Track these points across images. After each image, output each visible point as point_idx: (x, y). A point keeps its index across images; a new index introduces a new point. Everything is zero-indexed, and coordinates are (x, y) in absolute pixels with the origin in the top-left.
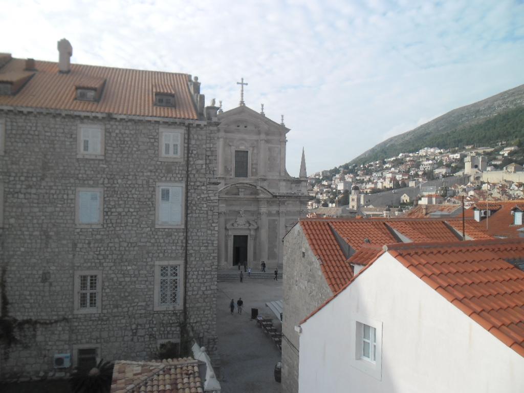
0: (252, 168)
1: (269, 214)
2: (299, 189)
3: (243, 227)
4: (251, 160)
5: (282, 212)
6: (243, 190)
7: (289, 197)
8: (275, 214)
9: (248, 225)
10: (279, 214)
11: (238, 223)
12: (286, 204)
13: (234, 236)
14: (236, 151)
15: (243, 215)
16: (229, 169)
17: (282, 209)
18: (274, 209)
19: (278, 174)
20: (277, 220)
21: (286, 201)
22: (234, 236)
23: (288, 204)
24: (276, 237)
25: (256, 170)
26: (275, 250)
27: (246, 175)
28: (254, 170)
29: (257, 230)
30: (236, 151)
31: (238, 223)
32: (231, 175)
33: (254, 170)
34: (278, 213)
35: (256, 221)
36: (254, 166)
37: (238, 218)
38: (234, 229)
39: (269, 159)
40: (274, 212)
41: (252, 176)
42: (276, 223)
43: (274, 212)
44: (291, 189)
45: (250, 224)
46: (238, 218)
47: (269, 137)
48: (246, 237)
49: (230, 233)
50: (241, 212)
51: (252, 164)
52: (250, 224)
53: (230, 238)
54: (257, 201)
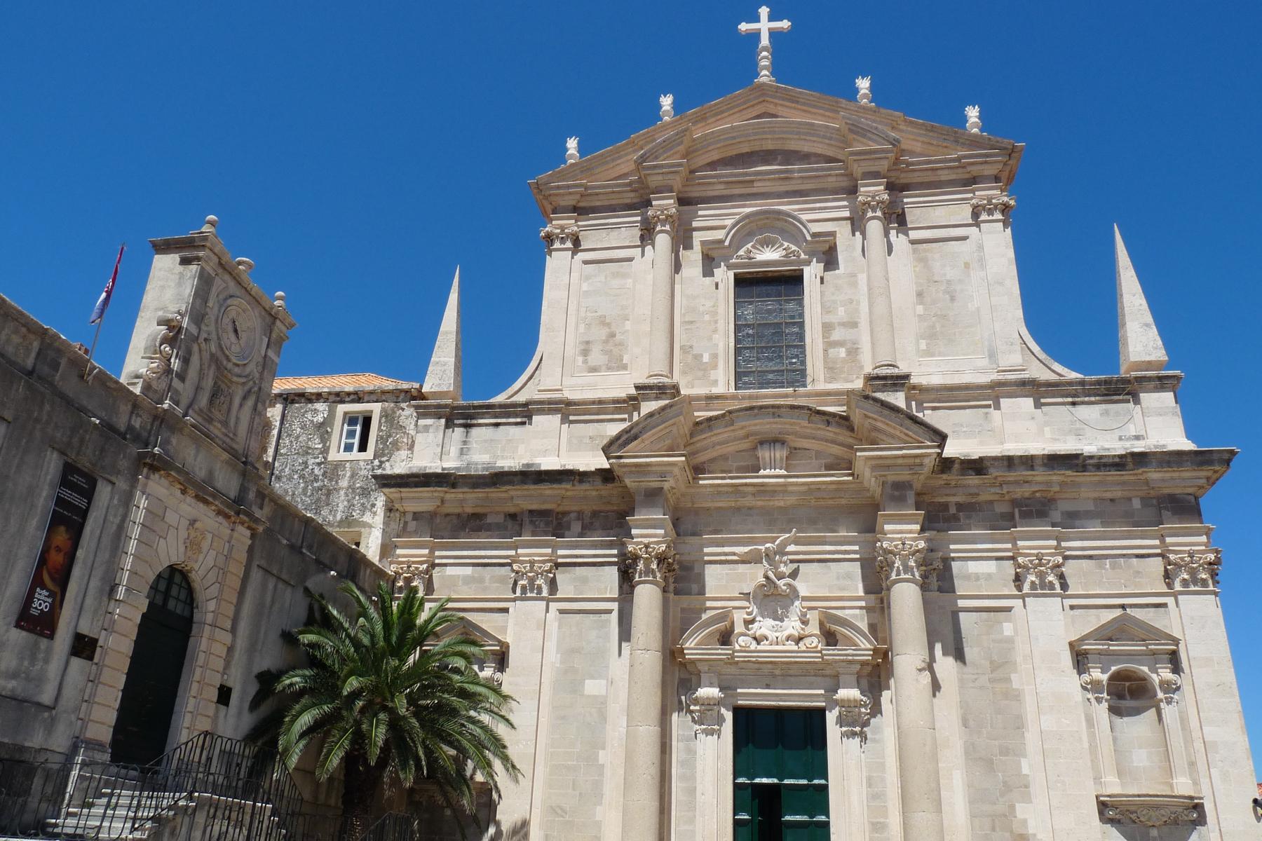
0: (829, 345)
2: (1132, 430)
4: (818, 308)
16: (706, 358)
19: (984, 362)
25: (853, 352)
26: (1021, 811)
27: (798, 376)
28: (842, 352)
32: (715, 382)
33: (842, 352)
36: (836, 335)
39: (920, 294)
41: (829, 380)
44: (1078, 434)
51: (827, 328)
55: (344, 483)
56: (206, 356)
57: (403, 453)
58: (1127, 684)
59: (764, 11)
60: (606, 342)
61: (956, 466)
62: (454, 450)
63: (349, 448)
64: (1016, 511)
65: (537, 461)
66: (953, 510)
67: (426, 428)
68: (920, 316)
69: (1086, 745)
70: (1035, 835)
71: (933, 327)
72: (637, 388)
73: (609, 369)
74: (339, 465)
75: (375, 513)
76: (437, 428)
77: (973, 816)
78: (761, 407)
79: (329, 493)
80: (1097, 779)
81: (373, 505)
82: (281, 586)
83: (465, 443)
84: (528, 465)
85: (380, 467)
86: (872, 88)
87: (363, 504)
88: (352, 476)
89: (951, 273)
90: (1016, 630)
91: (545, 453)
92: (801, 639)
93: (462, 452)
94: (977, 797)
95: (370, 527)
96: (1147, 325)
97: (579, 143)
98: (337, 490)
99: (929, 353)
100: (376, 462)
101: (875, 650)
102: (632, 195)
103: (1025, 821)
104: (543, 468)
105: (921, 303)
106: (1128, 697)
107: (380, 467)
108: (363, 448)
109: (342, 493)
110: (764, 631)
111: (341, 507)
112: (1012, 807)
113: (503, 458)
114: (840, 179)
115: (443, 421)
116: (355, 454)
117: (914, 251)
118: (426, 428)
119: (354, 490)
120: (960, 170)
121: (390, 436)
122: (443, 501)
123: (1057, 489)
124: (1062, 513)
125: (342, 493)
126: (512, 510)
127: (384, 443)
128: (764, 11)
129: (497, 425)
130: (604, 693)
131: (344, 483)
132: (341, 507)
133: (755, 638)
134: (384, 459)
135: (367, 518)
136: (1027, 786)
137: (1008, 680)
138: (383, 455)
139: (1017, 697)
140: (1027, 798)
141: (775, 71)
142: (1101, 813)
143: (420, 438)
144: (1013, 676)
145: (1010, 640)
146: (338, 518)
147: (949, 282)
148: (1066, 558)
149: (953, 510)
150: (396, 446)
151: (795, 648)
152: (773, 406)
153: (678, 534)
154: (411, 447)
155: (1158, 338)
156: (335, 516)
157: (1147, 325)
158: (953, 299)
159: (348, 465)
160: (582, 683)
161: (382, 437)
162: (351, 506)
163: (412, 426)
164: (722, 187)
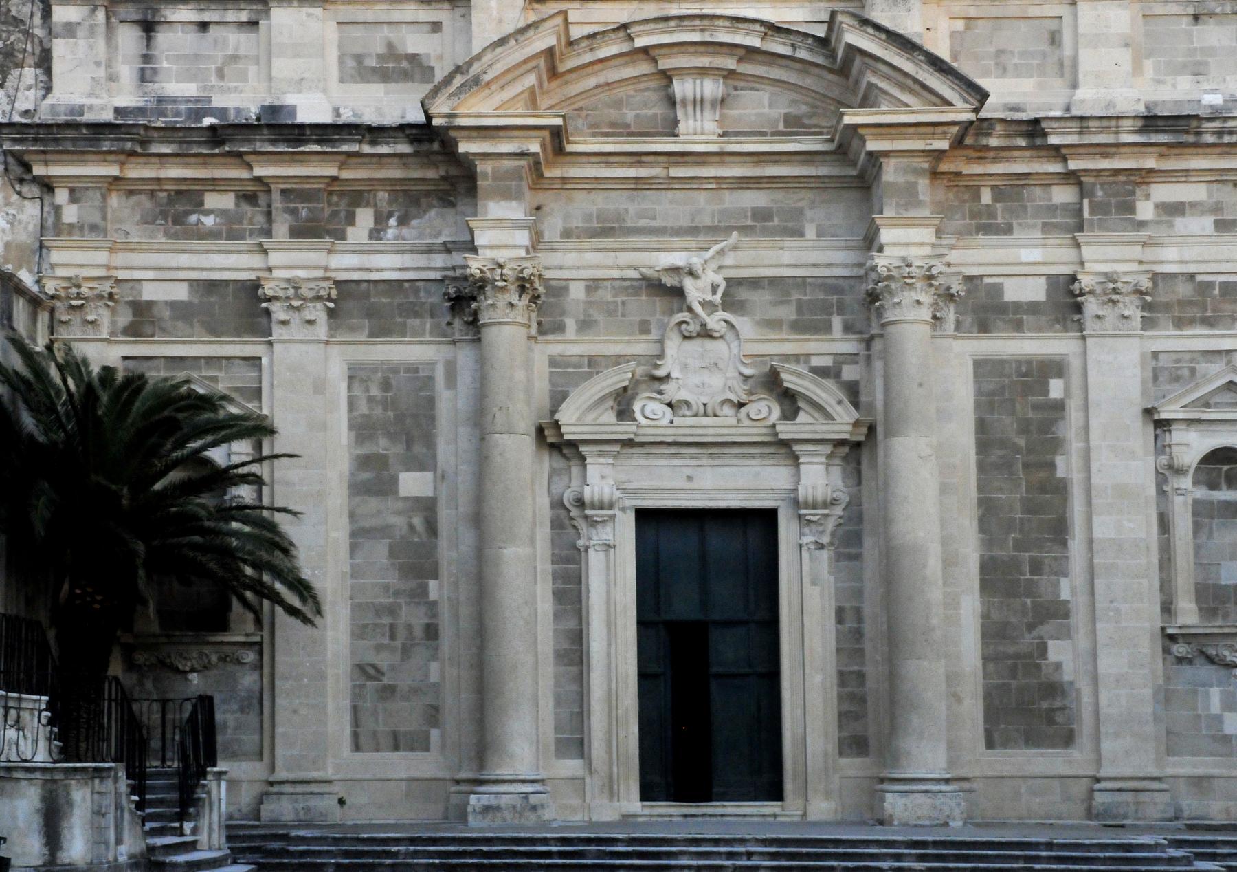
1: (983, 307)
3: (726, 425)
5: (1111, 291)
6: (711, 88)
7: (1172, 128)
8: (1033, 308)
9: (766, 409)
10: (1078, 308)
11: (672, 391)
12: (1145, 210)
13: (645, 517)
15: (715, 321)
17: (1105, 257)
18: (1022, 261)
21: (1145, 177)
22: (645, 517)
23: (1175, 209)
24: (1059, 531)
26: (1057, 651)
29: (858, 451)
31: (672, 391)
34: (1067, 302)
35: (849, 373)
37: (673, 345)
38: (629, 443)
40: (1035, 291)
42: (1056, 389)
43: (1035, 291)
44: (1198, 70)
45: (790, 401)
46: (673, 345)
49: (601, 479)
50: (695, 291)
52: (790, 401)
53: (604, 534)
54: (855, 175)
58: (1225, 468)
62: (127, 72)
64: (1086, 202)
65: (289, 99)
66: (986, 197)
67: (70, 30)
69: (1155, 560)
70: (1071, 683)
77: (986, 659)
80: (1167, 609)
83: (146, 58)
84: (273, 110)
90: (1067, 390)
91: (299, 84)
92: (741, 405)
93: (144, 77)
94: (993, 633)
101: (856, 424)
103: (1058, 666)
104: (303, 117)
106: (1224, 486)
110: (684, 395)
112: (1043, 649)
113: (222, 90)
115: (101, 15)
118: (70, 30)
124: (1157, 206)
129: (204, 26)
130: (429, 493)
133: (670, 405)
136: (1066, 616)
137: (1052, 466)
139: (1061, 489)
140: (1066, 634)
142: (1166, 651)
143: (59, 48)
144: (1059, 460)
145: (1059, 407)
148: (1155, 277)
151: (733, 421)
154: (45, 61)
160: (394, 481)
163: (37, 20)
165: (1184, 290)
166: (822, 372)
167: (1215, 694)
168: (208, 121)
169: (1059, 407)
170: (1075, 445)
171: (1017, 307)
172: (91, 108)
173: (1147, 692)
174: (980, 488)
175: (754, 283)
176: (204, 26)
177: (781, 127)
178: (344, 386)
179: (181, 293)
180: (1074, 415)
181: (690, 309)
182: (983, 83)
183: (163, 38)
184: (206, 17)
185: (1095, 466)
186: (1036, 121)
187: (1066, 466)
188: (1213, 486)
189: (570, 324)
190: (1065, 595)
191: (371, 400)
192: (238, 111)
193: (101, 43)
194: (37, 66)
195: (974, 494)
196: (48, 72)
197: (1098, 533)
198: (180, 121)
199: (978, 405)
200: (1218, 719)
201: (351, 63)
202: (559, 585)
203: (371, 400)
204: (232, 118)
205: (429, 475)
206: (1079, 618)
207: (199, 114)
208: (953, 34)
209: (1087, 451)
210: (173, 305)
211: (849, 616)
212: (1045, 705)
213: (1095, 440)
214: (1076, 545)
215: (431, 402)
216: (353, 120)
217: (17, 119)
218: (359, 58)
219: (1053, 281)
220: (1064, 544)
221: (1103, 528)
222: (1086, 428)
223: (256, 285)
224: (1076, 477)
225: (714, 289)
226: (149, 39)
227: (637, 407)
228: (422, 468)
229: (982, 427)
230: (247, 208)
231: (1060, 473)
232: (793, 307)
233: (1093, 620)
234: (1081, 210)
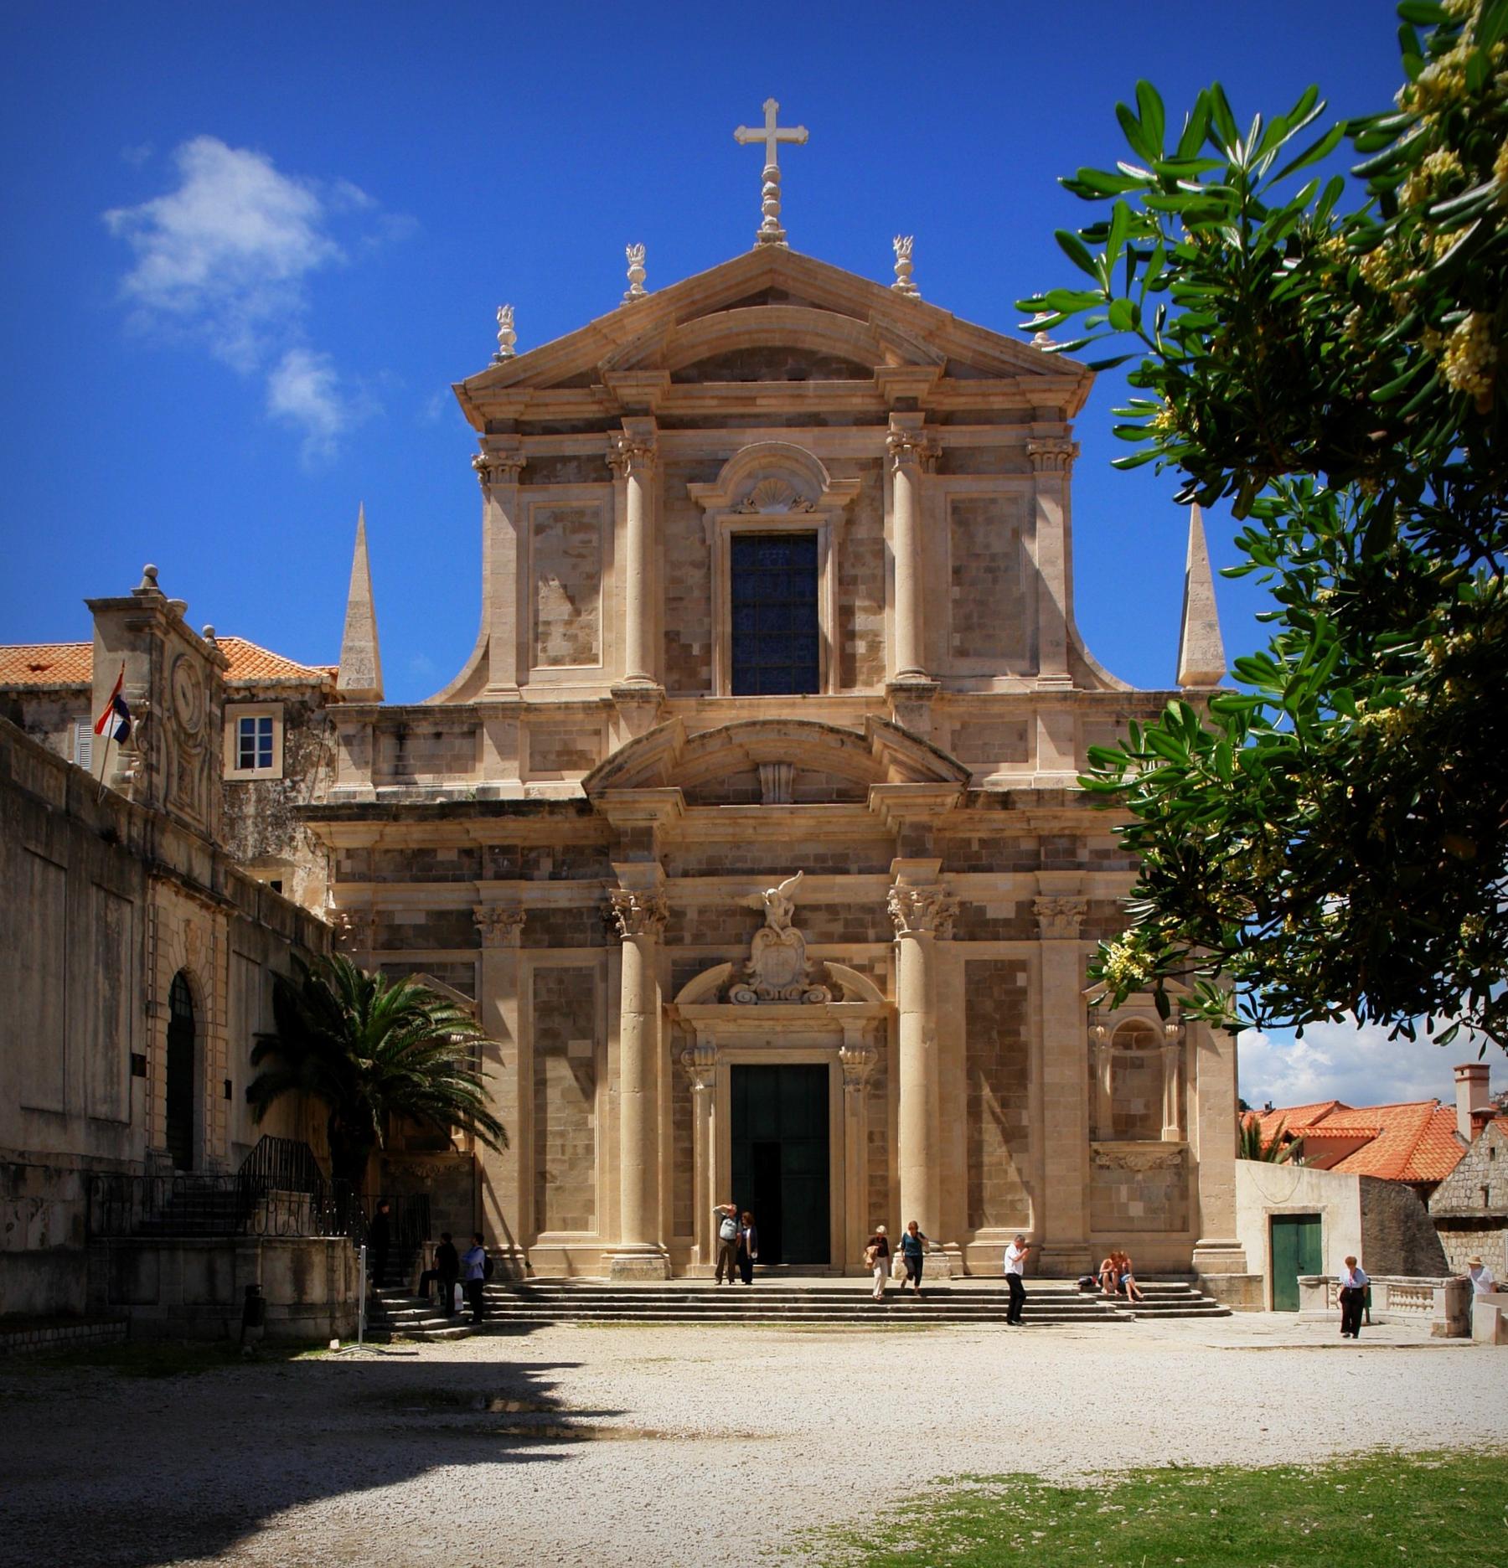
8: (1007, 922)
11: (756, 984)
12: (1083, 855)
14: (736, 539)
16: (696, 650)
20: (1022, 965)
30: (736, 539)
39: (957, 571)
42: (1021, 979)
43: (1007, 911)
47: (955, 437)
48: (820, 1073)
55: (250, 810)
56: (170, 735)
57: (322, 771)
59: (771, 107)
60: (569, 623)
61: (981, 800)
63: (247, 762)
65: (495, 783)
66: (975, 847)
68: (955, 601)
69: (1086, 1098)
71: (968, 617)
72: (615, 693)
73: (575, 661)
74: (237, 787)
75: (296, 849)
76: (363, 741)
78: (765, 723)
79: (232, 822)
81: (292, 838)
82: (251, 966)
83: (399, 758)
85: (293, 788)
86: (914, 257)
87: (278, 837)
88: (259, 801)
89: (998, 546)
90: (1029, 979)
95: (292, 865)
96: (1211, 626)
97: (515, 314)
98: (243, 818)
99: (962, 653)
100: (288, 783)
102: (595, 407)
105: (959, 584)
107: (293, 788)
108: (266, 761)
109: (250, 822)
110: (764, 986)
111: (251, 841)
114: (868, 400)
116: (257, 772)
117: (955, 510)
119: (264, 818)
120: (1018, 398)
121: (299, 747)
122: (381, 836)
123: (1088, 824)
124: (1091, 852)
125: (250, 822)
126: (468, 845)
127: (295, 756)
128: (771, 107)
131: (250, 810)
132: (251, 841)
134: (298, 778)
135: (286, 854)
136: (1026, 1137)
137: (1018, 1034)
138: (296, 773)
139: (1023, 1050)
141: (782, 219)
142: (1092, 1160)
144: (1023, 1029)
145: (1023, 992)
146: (250, 854)
147: (993, 557)
149: (975, 847)
150: (311, 762)
152: (779, 722)
153: (668, 876)
155: (1220, 643)
156: (245, 852)
157: (1211, 626)
158: (995, 581)
159: (251, 786)
161: (290, 749)
162: (263, 839)
164: (714, 402)
165: (1108, 911)
166: (861, 968)
167: (1124, 1190)
168: (439, 800)
169: (1023, 992)
170: (1033, 1018)
171: (996, 921)
172: (361, 793)
173: (1079, 1188)
174: (968, 1050)
175: (815, 908)
176: (438, 735)
177: (834, 797)
178: (531, 981)
179: (421, 920)
180: (1033, 997)
181: (770, 927)
182: (969, 768)
183: (410, 745)
184: (440, 729)
185: (1046, 1033)
186: (1007, 794)
187: (1028, 1033)
188: (1127, 1047)
189: (688, 937)
190: (1025, 1122)
191: (549, 991)
192: (461, 792)
193: (370, 749)
194: (328, 765)
195: (964, 1052)
196: (334, 770)
197: (1047, 1079)
198: (420, 801)
199: (967, 991)
200: (1126, 1205)
201: (538, 758)
202: (678, 1117)
203: (549, 991)
204: (456, 798)
205: (588, 1042)
206: (1033, 1139)
207: (434, 794)
208: (953, 732)
209: (1042, 1022)
210: (416, 927)
211: (876, 1137)
212: (1009, 1197)
213: (1046, 1016)
214: (1033, 1088)
215: (590, 992)
216: (539, 797)
217: (314, 803)
218: (544, 755)
219: (1019, 905)
220: (1026, 1088)
221: (1052, 1075)
222: (1041, 1006)
223: (472, 912)
224: (1034, 1041)
225: (786, 912)
226: (401, 744)
227: (732, 993)
228: (585, 1038)
229: (970, 1007)
230: (466, 860)
231: (1023, 1038)
232: (842, 922)
233: (1043, 1138)
234: (1038, 853)
